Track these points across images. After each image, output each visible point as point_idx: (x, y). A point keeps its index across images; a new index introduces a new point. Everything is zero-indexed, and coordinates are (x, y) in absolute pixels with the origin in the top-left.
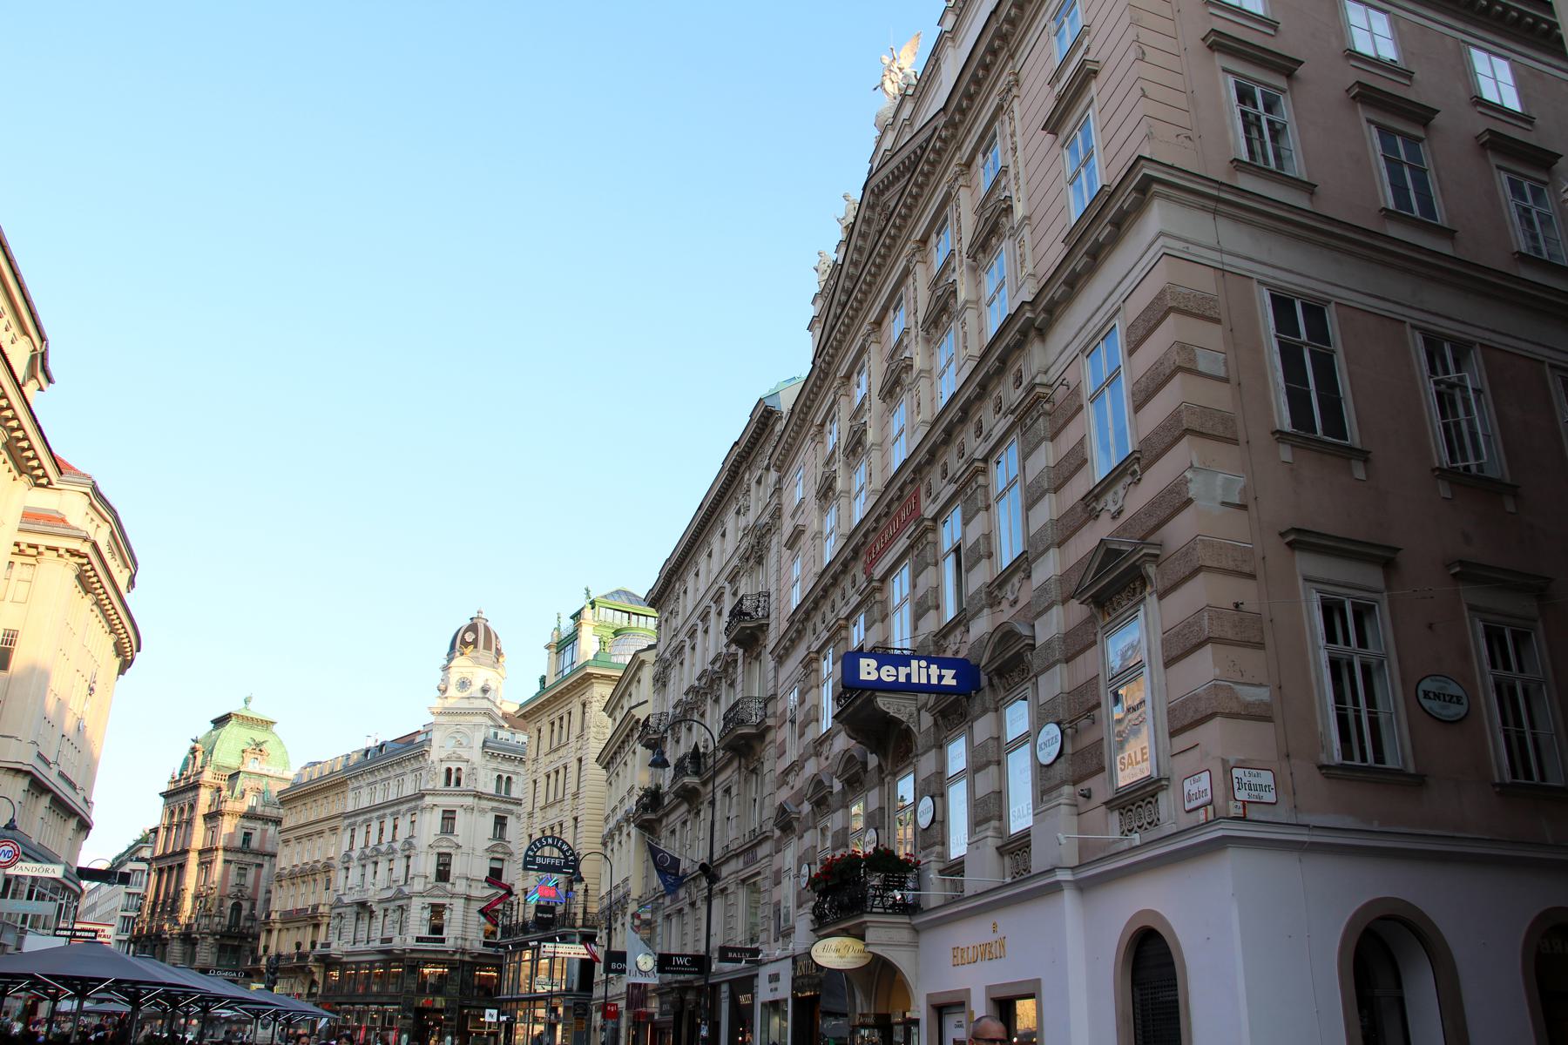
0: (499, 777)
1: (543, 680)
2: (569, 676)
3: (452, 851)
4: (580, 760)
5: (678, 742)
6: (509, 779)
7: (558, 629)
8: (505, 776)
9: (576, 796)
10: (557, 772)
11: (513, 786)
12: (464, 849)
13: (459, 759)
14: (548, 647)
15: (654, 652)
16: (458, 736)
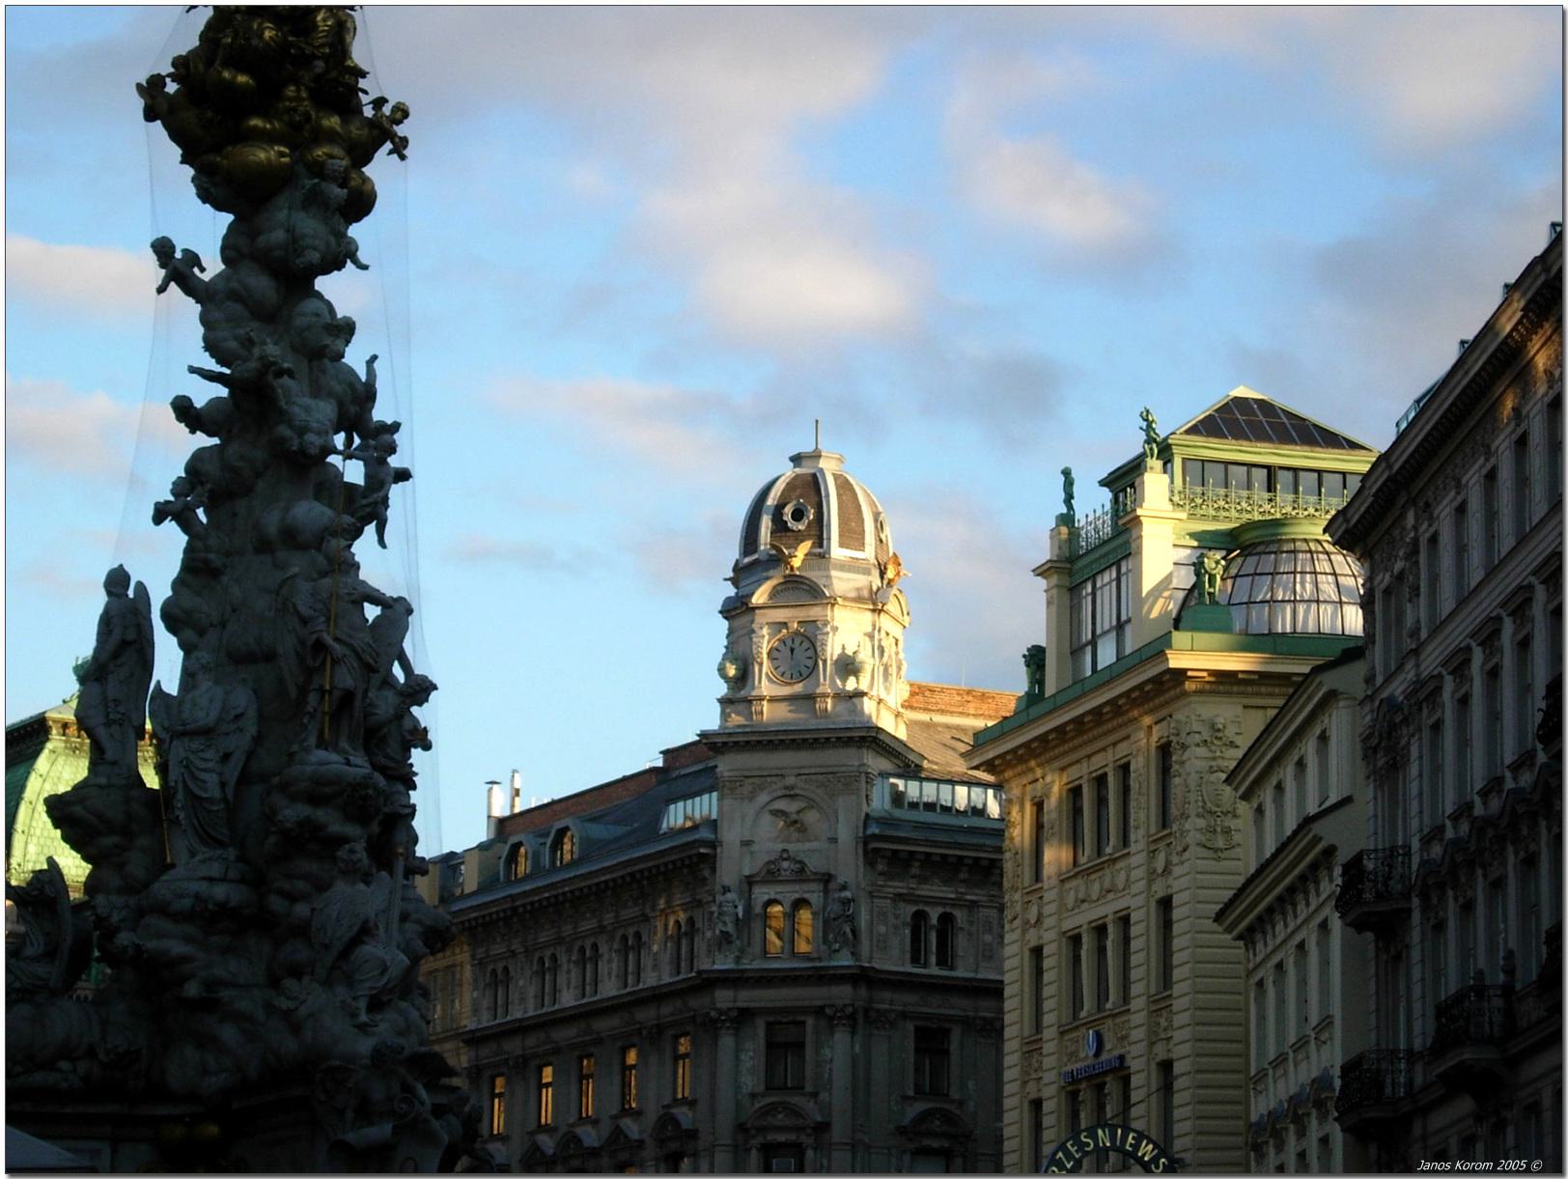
0: (920, 917)
1: (1035, 658)
2: (1113, 674)
3: (803, 1138)
4: (1166, 904)
5: (1440, 927)
6: (946, 919)
7: (1067, 519)
8: (934, 914)
9: (1161, 1003)
10: (1101, 930)
11: (961, 942)
12: (838, 1132)
13: (801, 874)
14: (1042, 572)
15: (1357, 670)
16: (791, 807)
